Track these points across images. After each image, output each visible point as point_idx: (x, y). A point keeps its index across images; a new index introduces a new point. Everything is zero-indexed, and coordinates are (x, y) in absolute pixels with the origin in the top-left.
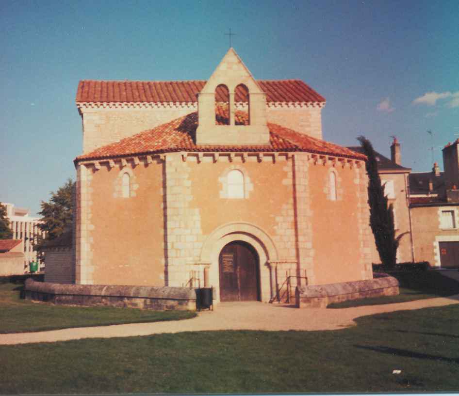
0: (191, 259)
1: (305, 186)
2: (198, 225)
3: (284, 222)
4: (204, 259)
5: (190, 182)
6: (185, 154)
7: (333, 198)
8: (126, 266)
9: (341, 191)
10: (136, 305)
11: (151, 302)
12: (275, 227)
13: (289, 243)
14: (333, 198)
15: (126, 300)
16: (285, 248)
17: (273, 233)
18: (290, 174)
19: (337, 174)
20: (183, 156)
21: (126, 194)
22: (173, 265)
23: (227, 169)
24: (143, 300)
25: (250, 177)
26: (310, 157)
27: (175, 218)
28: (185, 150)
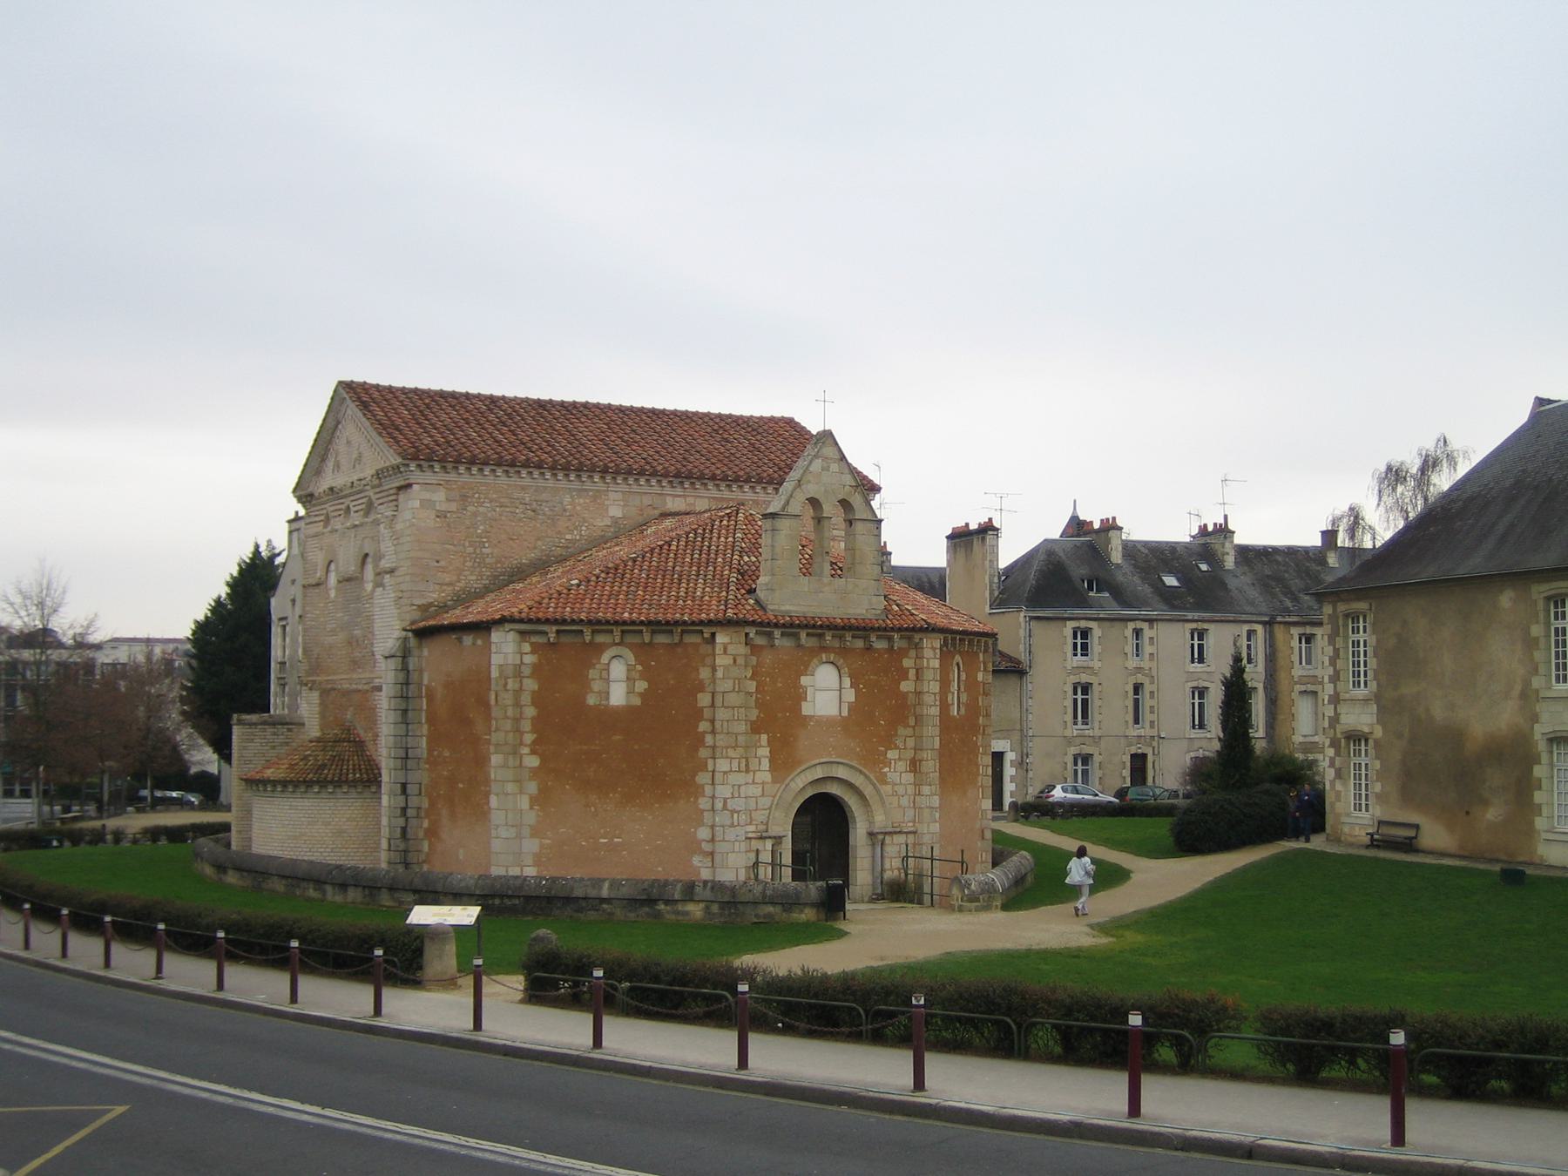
0: (752, 828)
2: (766, 764)
4: (775, 830)
6: (752, 631)
10: (687, 913)
11: (722, 908)
15: (661, 907)
18: (912, 673)
20: (747, 635)
21: (618, 696)
24: (702, 905)
27: (731, 753)
28: (753, 623)
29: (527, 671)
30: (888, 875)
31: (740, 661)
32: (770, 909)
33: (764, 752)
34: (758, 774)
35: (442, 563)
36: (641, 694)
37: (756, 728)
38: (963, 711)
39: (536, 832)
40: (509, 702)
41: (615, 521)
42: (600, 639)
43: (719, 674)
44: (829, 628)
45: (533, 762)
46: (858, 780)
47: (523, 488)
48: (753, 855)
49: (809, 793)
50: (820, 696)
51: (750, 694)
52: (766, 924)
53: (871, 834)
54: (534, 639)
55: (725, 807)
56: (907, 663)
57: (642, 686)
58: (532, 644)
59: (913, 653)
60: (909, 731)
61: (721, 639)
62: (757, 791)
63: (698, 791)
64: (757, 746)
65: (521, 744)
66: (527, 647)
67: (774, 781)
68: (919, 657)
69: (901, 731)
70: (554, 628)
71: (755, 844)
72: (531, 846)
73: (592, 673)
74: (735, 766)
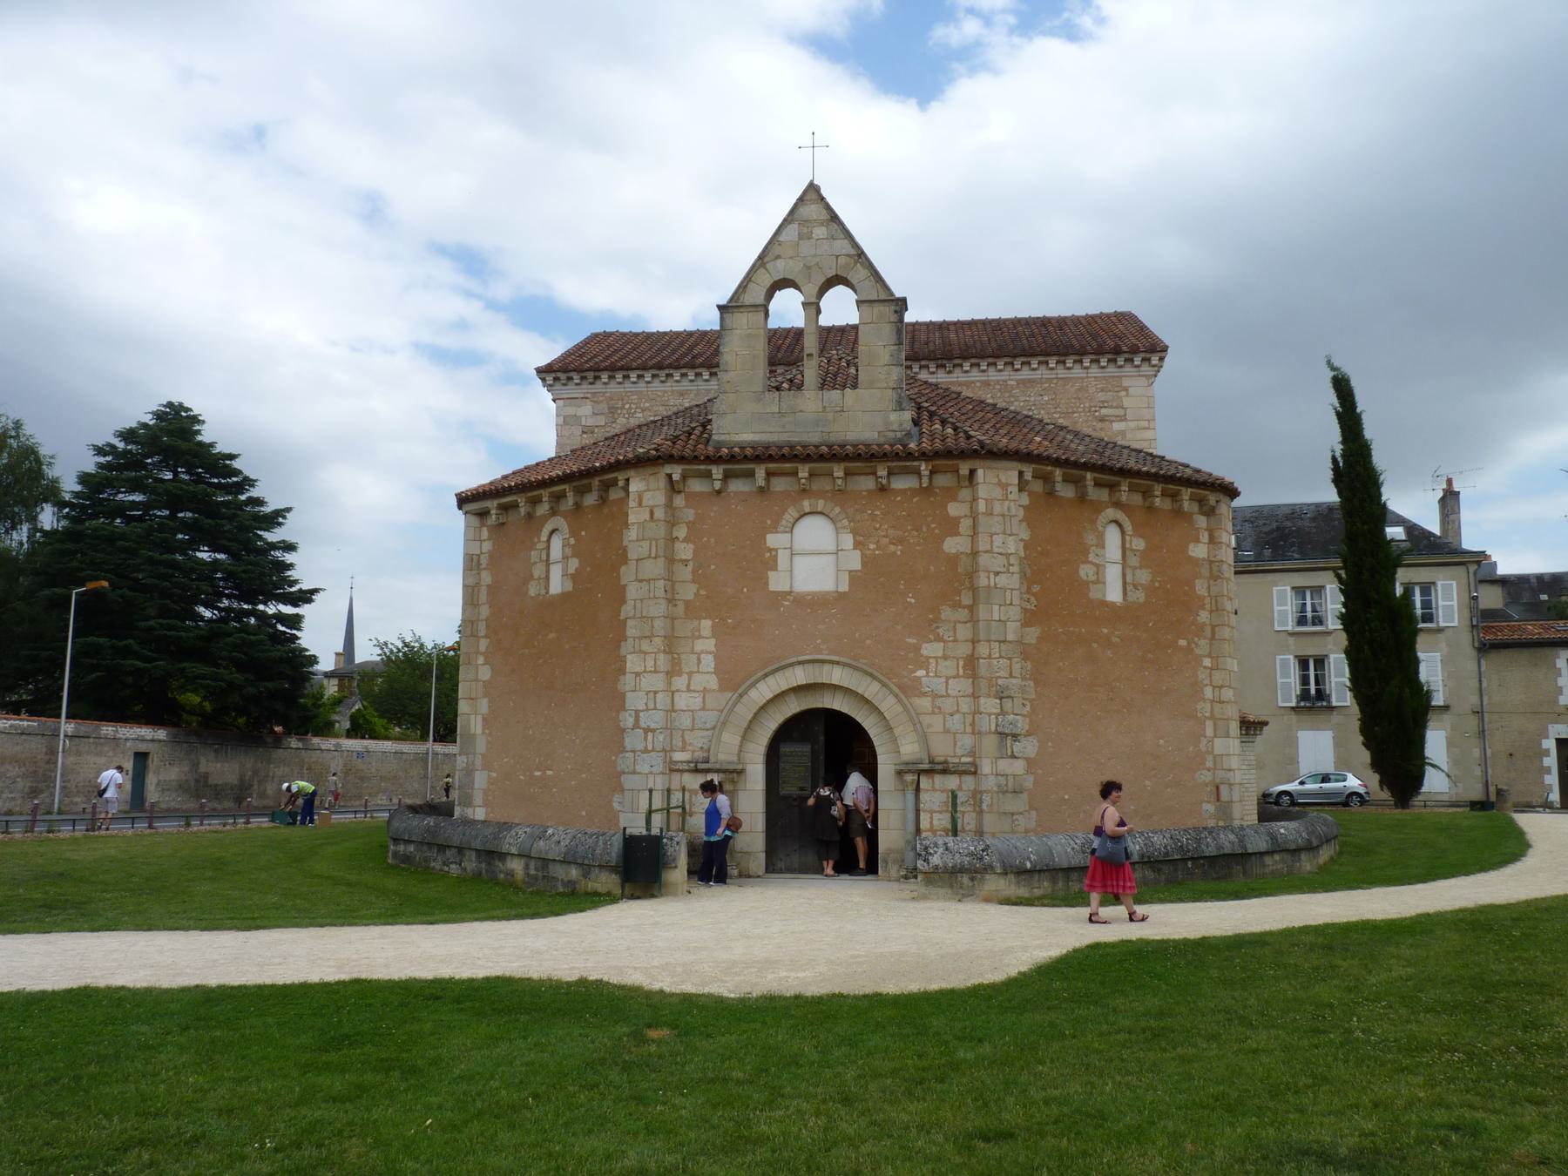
1: (1008, 555)
2: (708, 662)
3: (945, 657)
6: (676, 471)
7: (1114, 594)
9: (1144, 576)
13: (956, 717)
14: (1114, 594)
19: (1128, 527)
20: (670, 476)
21: (557, 585)
22: (634, 773)
23: (792, 513)
24: (523, 861)
25: (854, 532)
26: (1028, 476)
27: (645, 645)
29: (484, 561)
33: (707, 644)
34: (696, 678)
37: (693, 611)
39: (487, 766)
46: (870, 689)
49: (794, 707)
50: (801, 564)
51: (685, 562)
55: (636, 725)
56: (954, 509)
57: (574, 564)
60: (963, 614)
62: (697, 702)
63: (619, 701)
65: (478, 653)
66: (485, 533)
68: (975, 499)
69: (946, 613)
70: (495, 503)
74: (650, 664)
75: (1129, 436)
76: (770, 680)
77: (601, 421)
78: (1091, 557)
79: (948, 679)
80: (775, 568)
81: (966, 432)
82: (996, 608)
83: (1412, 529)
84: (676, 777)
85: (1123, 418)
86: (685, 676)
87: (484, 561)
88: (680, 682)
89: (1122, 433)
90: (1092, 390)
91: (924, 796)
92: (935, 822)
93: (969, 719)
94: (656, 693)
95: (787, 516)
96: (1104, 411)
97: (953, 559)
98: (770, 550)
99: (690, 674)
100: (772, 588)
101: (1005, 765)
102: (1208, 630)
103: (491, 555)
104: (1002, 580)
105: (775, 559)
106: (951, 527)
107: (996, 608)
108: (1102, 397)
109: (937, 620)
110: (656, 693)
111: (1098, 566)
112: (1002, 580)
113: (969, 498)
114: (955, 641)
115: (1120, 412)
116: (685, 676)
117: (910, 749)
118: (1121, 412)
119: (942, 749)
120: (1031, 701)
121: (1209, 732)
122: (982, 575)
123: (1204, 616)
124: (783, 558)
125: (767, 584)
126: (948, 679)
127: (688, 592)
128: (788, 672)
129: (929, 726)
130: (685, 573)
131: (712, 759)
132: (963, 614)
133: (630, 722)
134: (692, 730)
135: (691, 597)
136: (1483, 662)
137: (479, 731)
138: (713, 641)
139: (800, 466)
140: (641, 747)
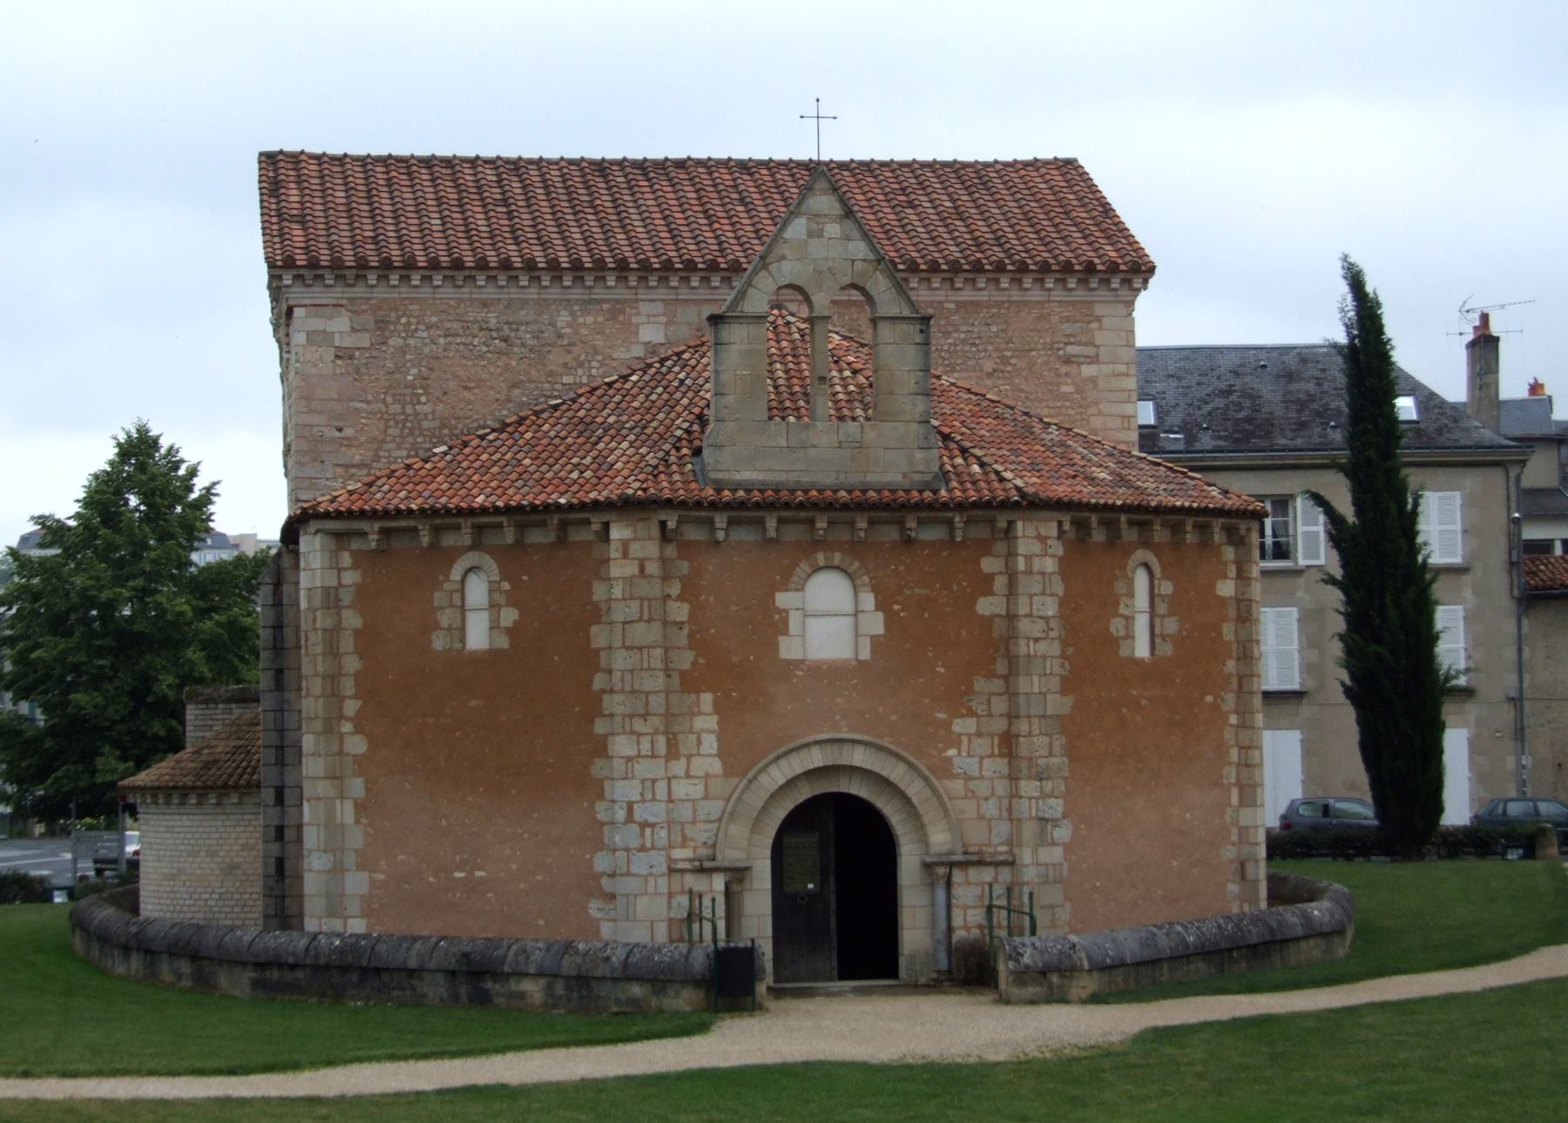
0: (687, 853)
1: (1046, 619)
2: (710, 744)
3: (979, 734)
4: (730, 855)
5: (686, 606)
7: (1142, 650)
8: (479, 874)
9: (1171, 626)
10: (522, 996)
11: (569, 989)
12: (951, 752)
13: (991, 801)
16: (981, 817)
17: (945, 769)
18: (1000, 583)
19: (1157, 570)
20: (663, 524)
21: (478, 636)
22: (628, 874)
23: (804, 567)
24: (542, 982)
25: (875, 590)
26: (1067, 526)
27: (638, 725)
29: (347, 598)
30: (959, 935)
31: (653, 568)
32: (636, 990)
33: (707, 722)
34: (696, 762)
35: (349, 432)
36: (509, 631)
37: (691, 683)
38: (1166, 649)
40: (319, 649)
41: (652, 348)
42: (448, 540)
43: (617, 592)
44: (771, 506)
45: (357, 745)
47: (485, 304)
48: (685, 900)
49: (805, 793)
50: (816, 627)
51: (679, 625)
52: (635, 1010)
53: (928, 867)
54: (356, 545)
56: (989, 565)
57: (509, 616)
58: (353, 554)
59: (1000, 547)
60: (998, 685)
61: (618, 533)
62: (697, 790)
63: (595, 789)
64: (694, 713)
65: (341, 717)
66: (346, 559)
67: (727, 773)
68: (1011, 554)
69: (980, 684)
70: (377, 526)
71: (691, 881)
72: (357, 883)
73: (439, 598)
74: (645, 747)
75: (1102, 384)
76: (783, 763)
77: (365, 340)
78: (1122, 609)
79: (982, 758)
80: (786, 632)
81: (997, 473)
82: (1036, 679)
83: (1428, 401)
84: (676, 878)
85: (1094, 360)
86: (683, 761)
87: (347, 598)
88: (678, 767)
89: (1093, 380)
90: (1055, 319)
91: (957, 891)
92: (969, 918)
93: (1005, 802)
94: (654, 781)
95: (798, 571)
96: (1071, 349)
97: (988, 621)
98: (780, 611)
99: (689, 757)
100: (784, 654)
101: (1045, 854)
102: (1235, 681)
103: (360, 590)
104: (1042, 648)
105: (785, 621)
106: (985, 585)
107: (1036, 679)
108: (1067, 328)
109: (969, 691)
110: (654, 781)
111: (1127, 618)
112: (1042, 648)
113: (1005, 552)
114: (990, 715)
115: (1090, 351)
116: (683, 761)
117: (940, 838)
118: (1090, 351)
119: (976, 836)
120: (1066, 779)
121: (1235, 800)
122: (1023, 642)
123: (1231, 666)
124: (794, 620)
125: (776, 650)
126: (982, 758)
127: (685, 659)
128: (804, 753)
129: (963, 812)
130: (682, 638)
131: (719, 857)
132: (998, 685)
133: (621, 814)
134: (694, 822)
135: (687, 666)
136: (1525, 622)
137: (349, 819)
138: (715, 718)
139: (818, 515)
140: (635, 843)
